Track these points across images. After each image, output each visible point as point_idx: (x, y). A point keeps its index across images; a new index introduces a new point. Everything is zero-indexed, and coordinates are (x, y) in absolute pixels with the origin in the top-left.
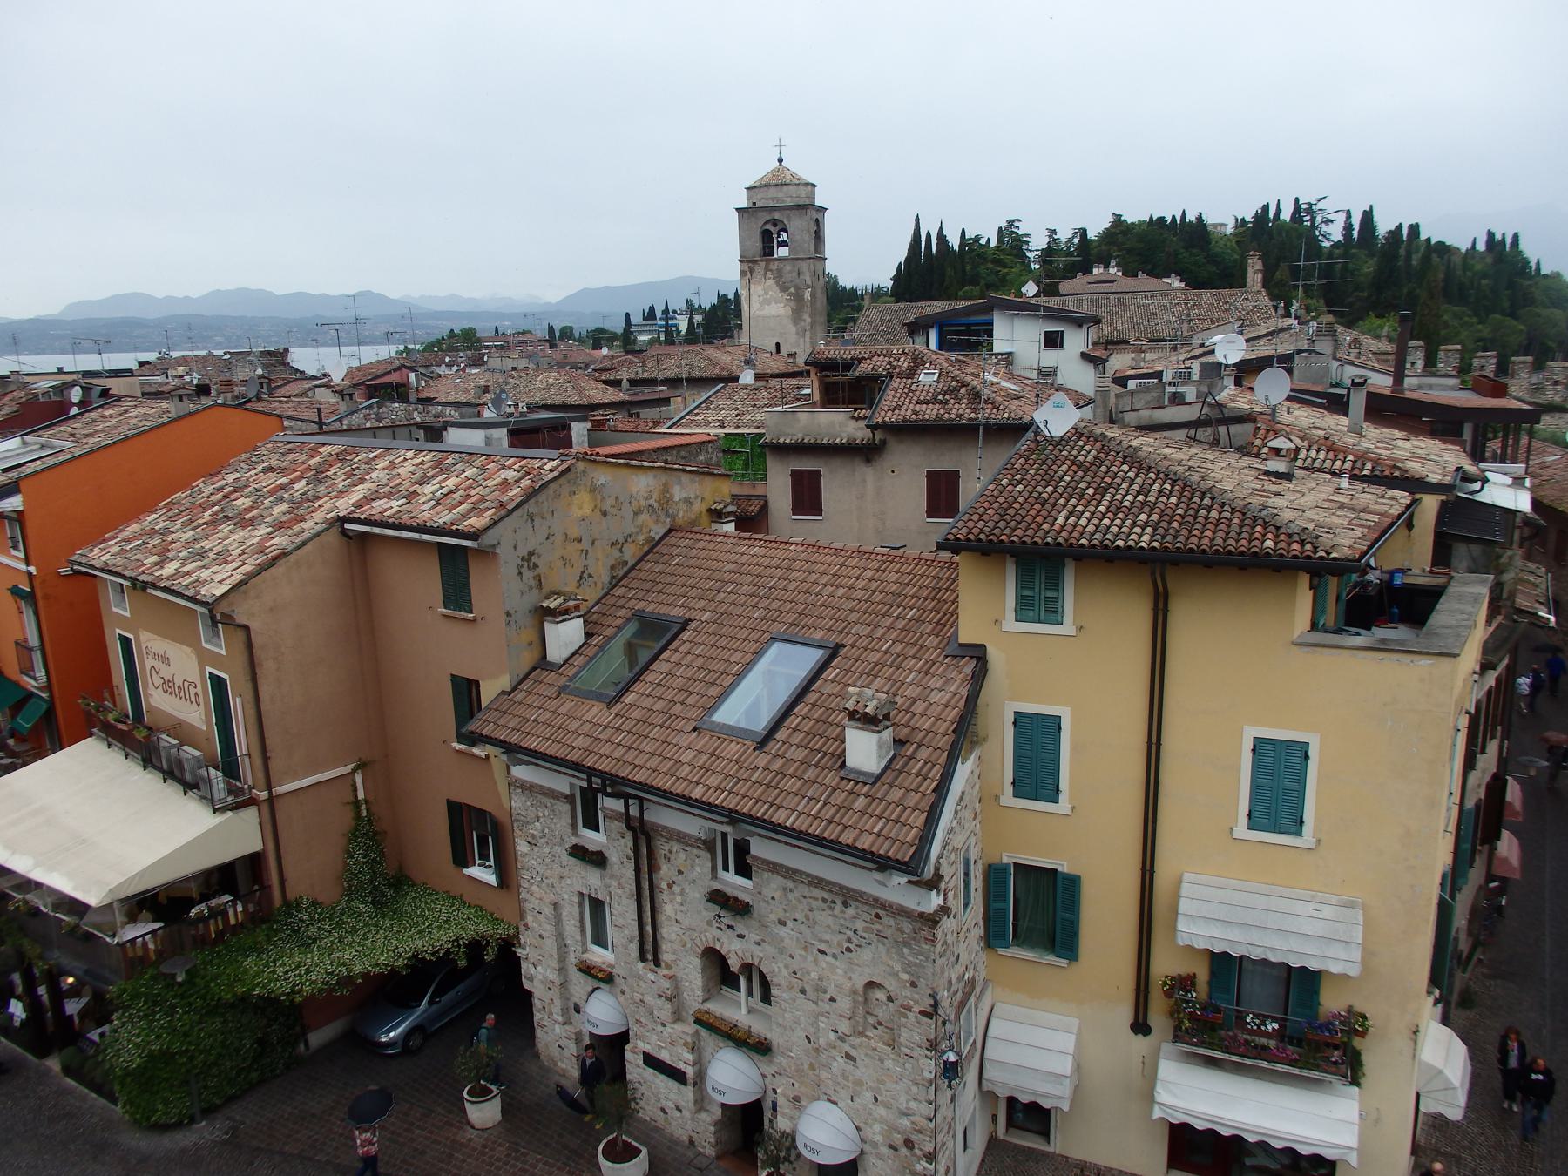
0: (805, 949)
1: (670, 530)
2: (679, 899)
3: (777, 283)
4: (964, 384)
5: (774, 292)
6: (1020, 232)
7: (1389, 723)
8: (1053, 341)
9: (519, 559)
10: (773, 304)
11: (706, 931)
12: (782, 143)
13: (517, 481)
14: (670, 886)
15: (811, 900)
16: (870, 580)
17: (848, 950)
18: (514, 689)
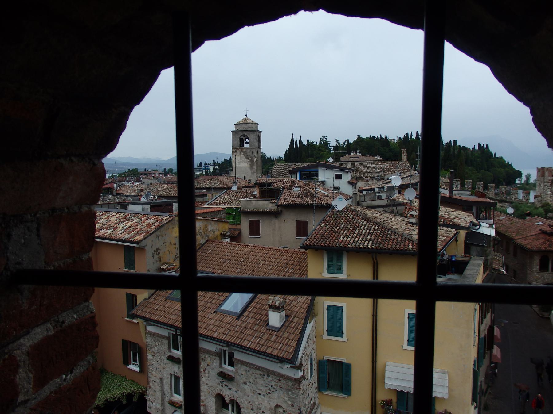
0: (254, 393)
1: (207, 241)
2: (207, 375)
3: (245, 156)
4: (309, 192)
5: (244, 159)
6: (327, 140)
7: (453, 308)
8: (339, 177)
9: (153, 251)
10: (243, 163)
11: (217, 387)
12: (247, 110)
13: (153, 224)
14: (204, 370)
15: (256, 375)
16: (277, 259)
17: (269, 393)
18: (149, 298)
